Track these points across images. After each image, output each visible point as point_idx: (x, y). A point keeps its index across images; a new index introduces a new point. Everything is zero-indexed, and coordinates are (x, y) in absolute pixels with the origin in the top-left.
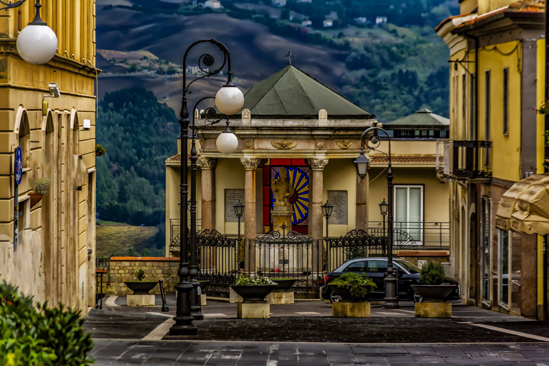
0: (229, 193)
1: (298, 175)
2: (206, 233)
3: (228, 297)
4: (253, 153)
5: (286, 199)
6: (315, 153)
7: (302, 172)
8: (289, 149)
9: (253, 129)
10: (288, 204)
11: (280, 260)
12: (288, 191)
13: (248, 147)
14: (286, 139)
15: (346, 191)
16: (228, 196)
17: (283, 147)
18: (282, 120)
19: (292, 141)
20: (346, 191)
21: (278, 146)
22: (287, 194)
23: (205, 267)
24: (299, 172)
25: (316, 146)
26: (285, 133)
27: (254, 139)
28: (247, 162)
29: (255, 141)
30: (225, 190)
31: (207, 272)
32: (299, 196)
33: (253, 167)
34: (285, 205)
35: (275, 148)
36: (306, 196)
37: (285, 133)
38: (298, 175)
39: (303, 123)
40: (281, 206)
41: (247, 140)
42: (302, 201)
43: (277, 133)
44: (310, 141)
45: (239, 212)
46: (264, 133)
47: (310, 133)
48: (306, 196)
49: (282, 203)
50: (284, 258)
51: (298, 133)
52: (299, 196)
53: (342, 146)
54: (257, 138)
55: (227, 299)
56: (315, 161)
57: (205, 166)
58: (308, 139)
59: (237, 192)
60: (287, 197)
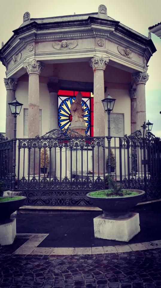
2: (54, 134)
9: (112, 25)
13: (101, 46)
15: (123, 114)
17: (127, 54)
20: (123, 114)
21: (123, 53)
28: (101, 60)
29: (107, 41)
35: (120, 54)
37: (131, 40)
40: (80, 121)
41: (98, 39)
43: (126, 38)
44: (140, 56)
47: (145, 47)
51: (138, 44)
57: (35, 69)
58: (139, 54)
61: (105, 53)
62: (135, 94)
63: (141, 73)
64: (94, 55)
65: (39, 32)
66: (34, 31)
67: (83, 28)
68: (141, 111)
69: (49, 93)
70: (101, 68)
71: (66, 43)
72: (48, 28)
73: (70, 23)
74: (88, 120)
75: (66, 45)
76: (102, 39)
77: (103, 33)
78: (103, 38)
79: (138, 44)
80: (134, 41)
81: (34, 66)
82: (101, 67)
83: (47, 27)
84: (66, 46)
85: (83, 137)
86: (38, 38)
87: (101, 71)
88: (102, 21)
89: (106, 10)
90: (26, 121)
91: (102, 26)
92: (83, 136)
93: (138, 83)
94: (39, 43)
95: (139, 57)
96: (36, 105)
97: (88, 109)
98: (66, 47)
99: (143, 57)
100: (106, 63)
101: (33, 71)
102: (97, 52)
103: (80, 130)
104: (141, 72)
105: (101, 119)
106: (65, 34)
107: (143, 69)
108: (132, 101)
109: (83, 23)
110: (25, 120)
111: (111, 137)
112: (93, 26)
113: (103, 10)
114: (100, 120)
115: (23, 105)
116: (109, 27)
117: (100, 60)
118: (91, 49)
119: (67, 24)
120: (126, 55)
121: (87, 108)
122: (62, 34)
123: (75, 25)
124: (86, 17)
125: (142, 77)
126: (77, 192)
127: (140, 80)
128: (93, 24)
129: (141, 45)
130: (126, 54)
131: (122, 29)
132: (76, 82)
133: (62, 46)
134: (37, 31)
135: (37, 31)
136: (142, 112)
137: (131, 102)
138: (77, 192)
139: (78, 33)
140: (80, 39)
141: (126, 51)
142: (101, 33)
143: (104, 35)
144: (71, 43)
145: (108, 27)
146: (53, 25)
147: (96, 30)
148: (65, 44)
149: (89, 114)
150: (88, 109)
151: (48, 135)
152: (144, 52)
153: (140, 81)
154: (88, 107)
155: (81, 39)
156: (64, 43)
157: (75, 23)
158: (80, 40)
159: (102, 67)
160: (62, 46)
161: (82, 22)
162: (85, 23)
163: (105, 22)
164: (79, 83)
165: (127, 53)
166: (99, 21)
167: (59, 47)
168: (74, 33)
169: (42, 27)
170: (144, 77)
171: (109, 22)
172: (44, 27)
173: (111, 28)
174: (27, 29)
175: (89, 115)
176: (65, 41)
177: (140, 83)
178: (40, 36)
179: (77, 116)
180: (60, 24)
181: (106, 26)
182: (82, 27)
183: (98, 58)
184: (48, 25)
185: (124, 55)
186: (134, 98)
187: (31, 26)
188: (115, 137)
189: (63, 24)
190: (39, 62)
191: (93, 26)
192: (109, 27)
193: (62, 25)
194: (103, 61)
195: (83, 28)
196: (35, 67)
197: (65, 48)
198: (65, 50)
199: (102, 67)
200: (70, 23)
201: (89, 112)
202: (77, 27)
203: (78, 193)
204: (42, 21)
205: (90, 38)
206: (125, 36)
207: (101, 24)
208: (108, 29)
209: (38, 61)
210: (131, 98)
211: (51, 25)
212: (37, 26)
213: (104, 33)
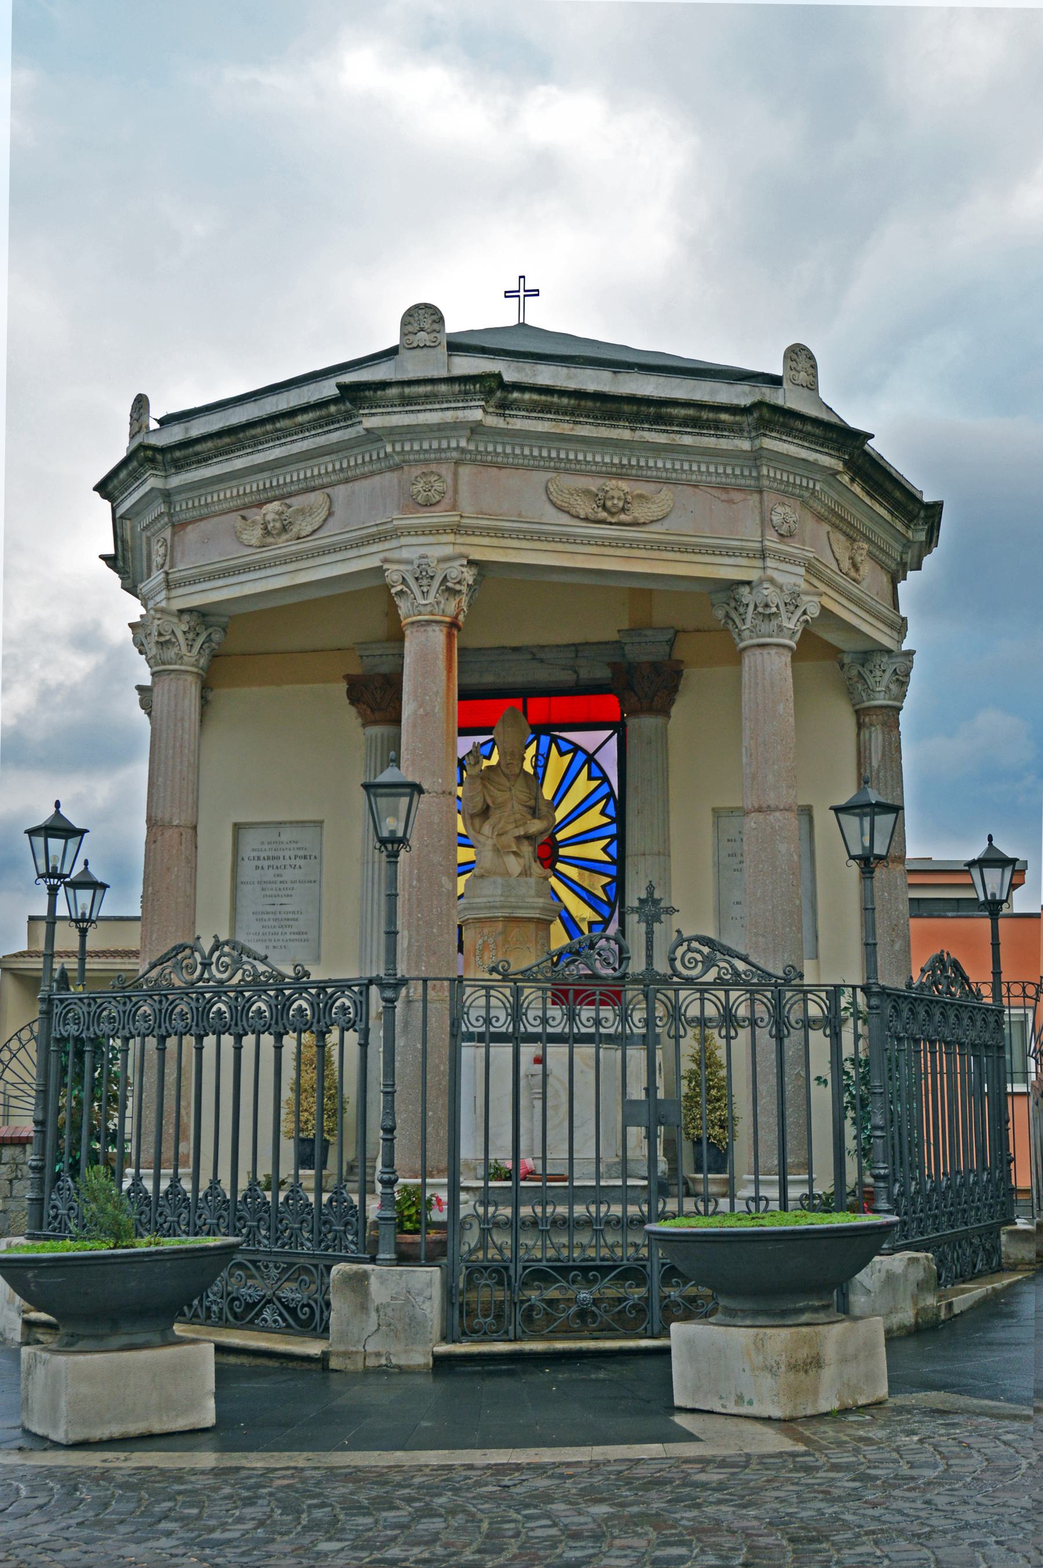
0: (251, 840)
1: (557, 764)
2: (179, 967)
3: (324, 1332)
4: (457, 530)
5: (527, 849)
6: (763, 554)
7: (576, 749)
8: (635, 524)
10: (537, 868)
11: (629, 1106)
12: (534, 812)
13: (428, 504)
14: (620, 473)
16: (246, 851)
17: (608, 511)
18: (606, 375)
19: (652, 487)
21: (585, 507)
22: (536, 826)
23: (168, 1153)
24: (562, 754)
25: (765, 522)
26: (626, 434)
27: (457, 463)
30: (237, 827)
31: (176, 1179)
32: (562, 852)
33: (451, 607)
34: (525, 873)
35: (565, 519)
36: (594, 851)
37: (626, 434)
38: (557, 764)
39: (713, 392)
40: (507, 874)
41: (417, 471)
42: (572, 872)
44: (736, 496)
45: (391, 825)
46: (518, 424)
47: (745, 445)
48: (594, 851)
49: (514, 865)
50: (651, 1089)
52: (562, 852)
53: (846, 565)
54: (473, 461)
55: (314, 1348)
56: (768, 592)
57: (171, 653)
58: (724, 488)
59: (287, 835)
60: (529, 838)
61: (451, 538)
62: (871, 681)
63: (745, 590)
64: (382, 556)
65: (176, 481)
66: (152, 482)
67: (335, 437)
68: (756, 806)
69: (360, 730)
70: (427, 617)
71: (276, 513)
72: (203, 460)
73: (278, 425)
74: (607, 859)
75: (278, 525)
76: (434, 467)
77: (435, 438)
78: (439, 461)
79: (687, 440)
80: (650, 430)
81: (162, 639)
82: (421, 609)
83: (197, 454)
84: (284, 526)
85: (287, 980)
86: (178, 509)
87: (429, 629)
88: (407, 390)
89: (436, 326)
90: (246, 890)
91: (412, 411)
92: (284, 977)
93: (742, 645)
94: (190, 527)
95: (731, 501)
96: (170, 822)
97: (610, 795)
98: (284, 529)
99: (761, 492)
100: (449, 584)
101: (163, 663)
102: (404, 540)
103: (500, 926)
104: (749, 583)
105: (419, 880)
106: (278, 471)
107: (758, 563)
108: (860, 726)
109: (330, 415)
110: (238, 881)
111: (404, 982)
112: (369, 423)
113: (422, 330)
114: (415, 883)
115: (87, 831)
116: (453, 405)
117: (417, 579)
118: (381, 528)
119: (269, 427)
120: (603, 515)
121: (605, 790)
122: (266, 474)
123: (302, 428)
124: (329, 389)
125: (751, 607)
126: (249, 1261)
127: (748, 625)
128: (366, 411)
129: (709, 442)
130: (604, 507)
131: (543, 398)
132: (515, 649)
133: (266, 528)
134: (166, 477)
135: (166, 477)
136: (759, 810)
137: (858, 735)
138: (249, 1261)
139: (327, 458)
140: (340, 482)
141: (601, 495)
142: (421, 440)
143: (440, 450)
144: (302, 511)
145: (448, 409)
146: (219, 442)
147: (392, 432)
148: (274, 520)
149: (613, 821)
150: (610, 795)
151: (154, 973)
152: (758, 468)
153: (747, 632)
154: (605, 779)
155: (347, 481)
156: (270, 517)
157: (300, 419)
158: (342, 487)
159: (429, 608)
160: (267, 532)
161: (324, 412)
162: (339, 412)
163: (422, 390)
164: (534, 654)
165: (609, 503)
166: (393, 392)
167: (254, 535)
168: (311, 463)
169: (179, 460)
170: (760, 610)
171: (443, 388)
172: (185, 458)
173: (464, 408)
174: (130, 475)
175: (613, 829)
176: (276, 506)
177: (755, 641)
178: (184, 496)
179: (490, 848)
180: (241, 435)
181: (437, 406)
182: (329, 431)
183: (409, 567)
184: (198, 448)
185: (591, 516)
186: (869, 708)
187: (135, 464)
188: (425, 981)
189: (253, 432)
190: (186, 617)
191: (369, 423)
192: (453, 405)
193: (253, 437)
194: (432, 577)
195: (335, 437)
196: (168, 642)
197: (279, 534)
198: (284, 546)
199: (429, 608)
200: (278, 425)
201: (611, 810)
202: (313, 432)
203: (254, 1262)
204: (187, 430)
205: (381, 472)
206: (576, 423)
207: (406, 401)
208: (449, 416)
209: (181, 612)
210: (853, 705)
211: (210, 444)
212: (159, 457)
213: (439, 439)
